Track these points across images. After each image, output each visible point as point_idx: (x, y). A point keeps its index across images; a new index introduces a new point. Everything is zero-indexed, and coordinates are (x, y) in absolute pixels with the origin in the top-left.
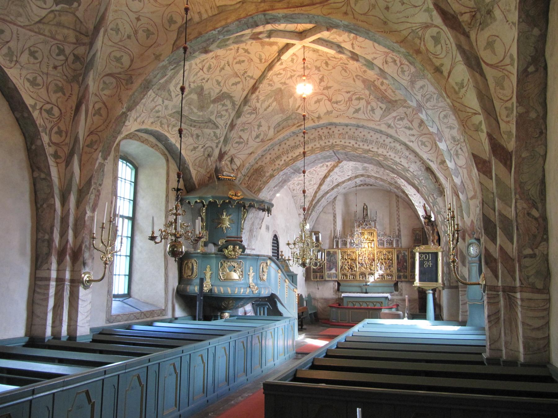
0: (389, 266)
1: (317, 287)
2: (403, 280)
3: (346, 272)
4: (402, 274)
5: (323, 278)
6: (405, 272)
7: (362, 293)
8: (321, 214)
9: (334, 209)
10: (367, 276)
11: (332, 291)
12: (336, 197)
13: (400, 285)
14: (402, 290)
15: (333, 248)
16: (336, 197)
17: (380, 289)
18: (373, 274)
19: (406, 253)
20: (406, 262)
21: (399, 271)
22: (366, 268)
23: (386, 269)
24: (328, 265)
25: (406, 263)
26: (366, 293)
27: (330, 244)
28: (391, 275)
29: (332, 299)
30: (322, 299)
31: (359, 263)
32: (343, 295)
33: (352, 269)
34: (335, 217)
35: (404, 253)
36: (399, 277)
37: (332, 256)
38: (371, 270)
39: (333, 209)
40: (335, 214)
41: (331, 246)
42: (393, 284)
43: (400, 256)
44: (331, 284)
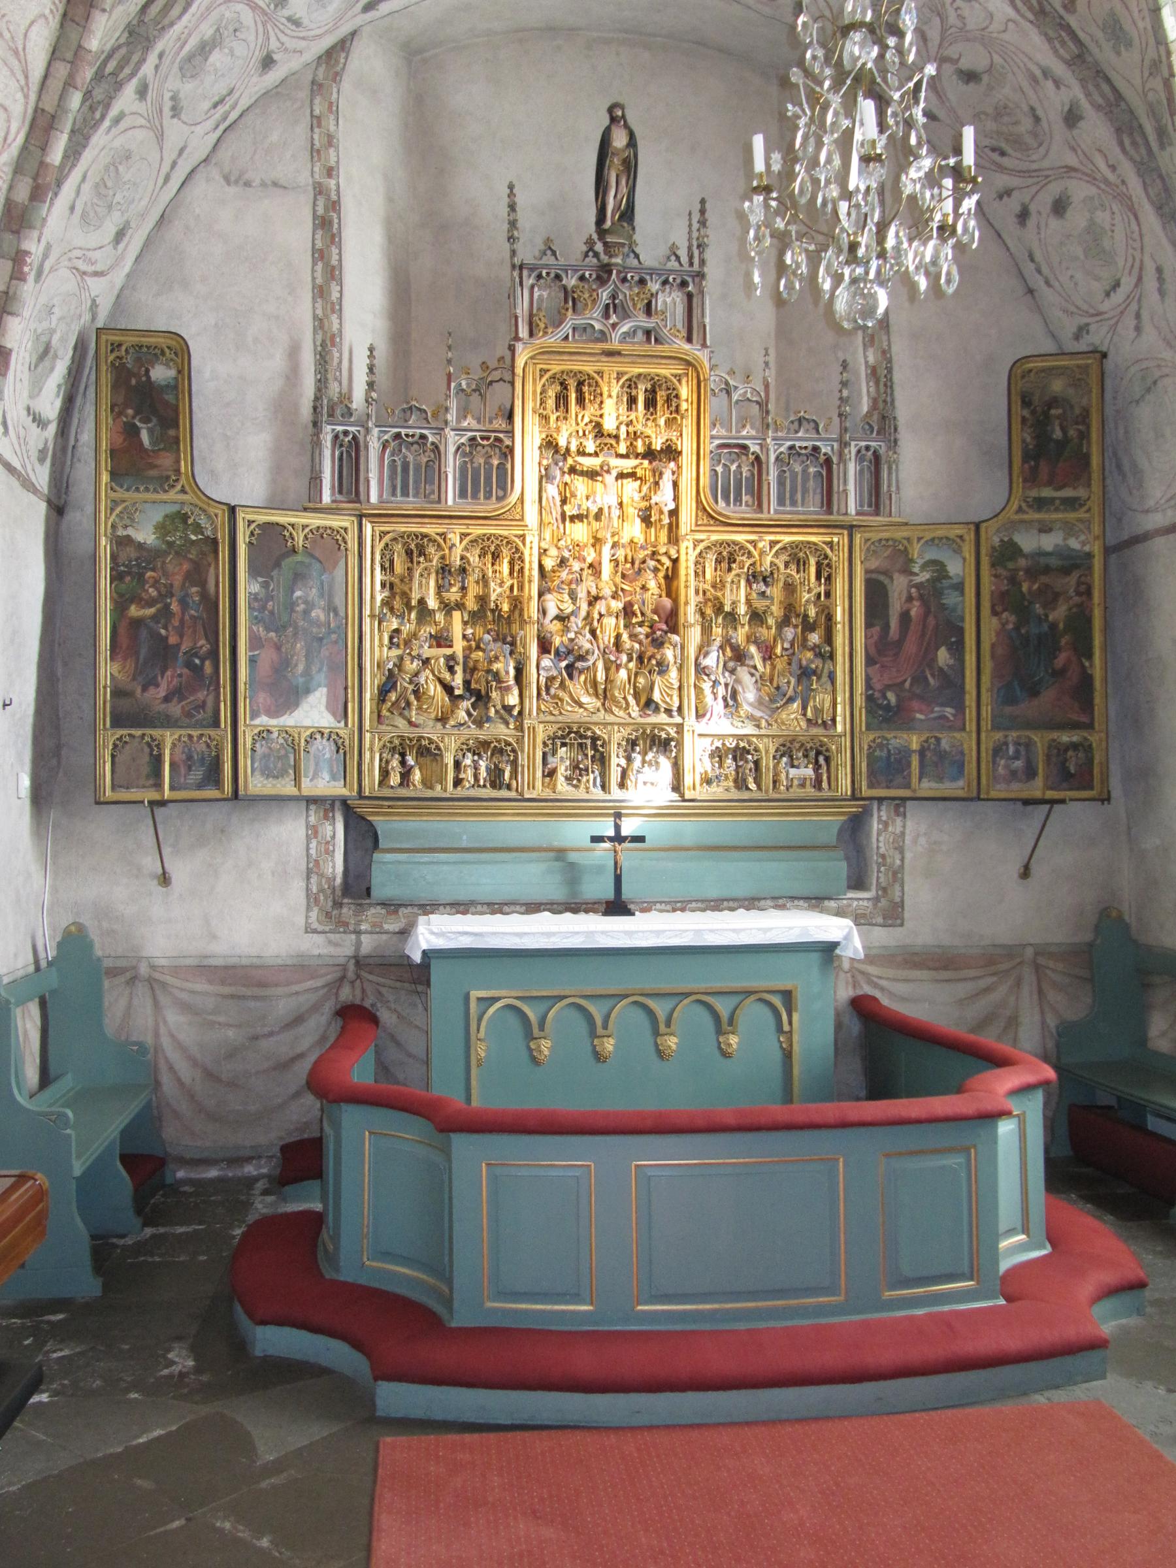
0: (805, 674)
1: (150, 863)
2: (927, 787)
3: (431, 731)
4: (915, 742)
5: (213, 775)
6: (942, 723)
7: (575, 907)
8: (205, 191)
9: (322, 149)
10: (617, 761)
11: (297, 891)
12: (343, 45)
13: (880, 831)
14: (897, 875)
15: (311, 504)
16: (343, 45)
17: (740, 873)
18: (664, 745)
19: (954, 568)
20: (952, 634)
21: (882, 712)
22: (605, 695)
23: (775, 699)
24: (267, 657)
25: (958, 649)
26: (617, 907)
27: (277, 469)
28: (820, 755)
29: (301, 968)
30: (206, 970)
31: (544, 646)
32: (434, 933)
33: (481, 699)
34: (327, 225)
35: (939, 568)
36: (887, 768)
37: (298, 577)
38: (649, 704)
39: (315, 153)
40: (335, 206)
41: (297, 487)
42: (831, 822)
43: (898, 587)
44: (289, 834)
